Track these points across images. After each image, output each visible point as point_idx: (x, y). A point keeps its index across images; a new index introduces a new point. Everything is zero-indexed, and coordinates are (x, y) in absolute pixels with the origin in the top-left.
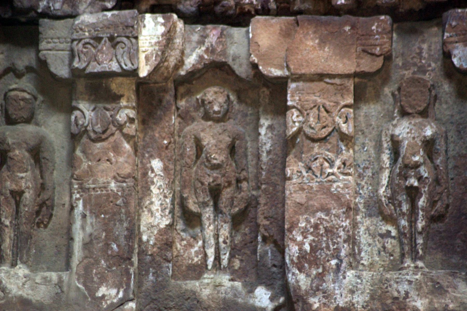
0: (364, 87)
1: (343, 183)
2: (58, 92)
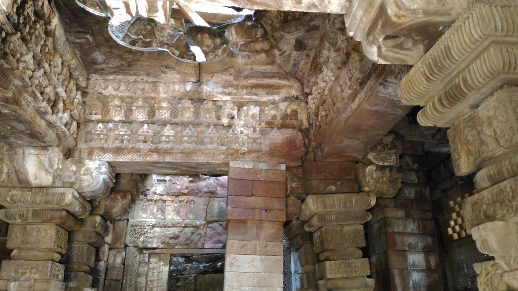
0: (173, 201)
1: (170, 209)
2: (148, 201)
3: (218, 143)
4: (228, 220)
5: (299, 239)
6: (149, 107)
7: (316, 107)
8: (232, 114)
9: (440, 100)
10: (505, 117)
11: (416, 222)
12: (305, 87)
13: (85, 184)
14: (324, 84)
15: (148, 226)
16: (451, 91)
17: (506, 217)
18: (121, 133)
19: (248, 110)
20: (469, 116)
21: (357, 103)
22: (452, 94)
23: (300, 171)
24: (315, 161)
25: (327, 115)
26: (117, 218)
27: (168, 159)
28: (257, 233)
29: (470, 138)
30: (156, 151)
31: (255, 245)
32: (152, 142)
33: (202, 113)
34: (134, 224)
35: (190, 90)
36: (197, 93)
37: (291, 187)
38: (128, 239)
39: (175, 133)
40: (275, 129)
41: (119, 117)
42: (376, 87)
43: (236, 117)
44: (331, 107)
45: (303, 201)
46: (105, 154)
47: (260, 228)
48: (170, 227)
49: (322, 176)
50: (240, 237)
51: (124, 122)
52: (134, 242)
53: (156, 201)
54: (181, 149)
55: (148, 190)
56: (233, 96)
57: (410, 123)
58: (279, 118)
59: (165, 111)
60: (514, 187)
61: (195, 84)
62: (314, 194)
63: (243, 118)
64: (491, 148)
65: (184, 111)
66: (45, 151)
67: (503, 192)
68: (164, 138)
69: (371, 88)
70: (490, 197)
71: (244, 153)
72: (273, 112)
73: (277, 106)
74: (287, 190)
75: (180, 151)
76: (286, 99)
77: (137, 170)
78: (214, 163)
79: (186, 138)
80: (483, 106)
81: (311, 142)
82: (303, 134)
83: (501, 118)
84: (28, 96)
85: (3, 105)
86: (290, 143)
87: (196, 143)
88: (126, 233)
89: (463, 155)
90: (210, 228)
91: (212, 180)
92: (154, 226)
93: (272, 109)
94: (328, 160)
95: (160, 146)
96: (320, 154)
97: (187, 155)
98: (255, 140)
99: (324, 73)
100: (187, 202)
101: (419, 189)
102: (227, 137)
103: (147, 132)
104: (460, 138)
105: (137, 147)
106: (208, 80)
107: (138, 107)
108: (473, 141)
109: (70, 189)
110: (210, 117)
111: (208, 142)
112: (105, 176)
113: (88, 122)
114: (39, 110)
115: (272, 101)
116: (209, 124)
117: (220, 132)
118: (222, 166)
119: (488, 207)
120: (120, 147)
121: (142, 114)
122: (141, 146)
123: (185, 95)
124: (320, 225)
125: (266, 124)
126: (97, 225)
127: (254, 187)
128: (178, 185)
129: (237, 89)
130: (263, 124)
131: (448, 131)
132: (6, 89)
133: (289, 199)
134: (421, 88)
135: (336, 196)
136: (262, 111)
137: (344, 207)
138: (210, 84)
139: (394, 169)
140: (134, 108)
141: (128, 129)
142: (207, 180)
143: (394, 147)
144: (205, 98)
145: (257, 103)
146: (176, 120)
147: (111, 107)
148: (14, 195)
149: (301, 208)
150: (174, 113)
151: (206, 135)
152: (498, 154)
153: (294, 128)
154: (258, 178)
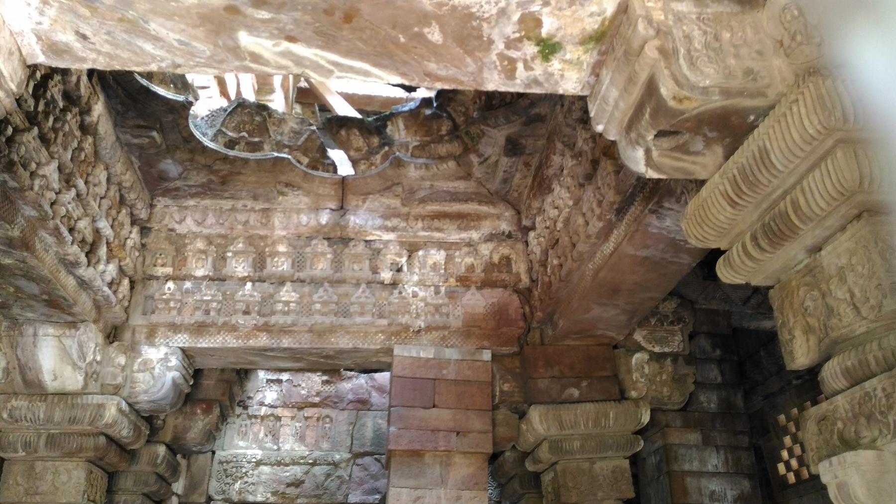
0: (293, 418)
1: (288, 432)
2: (250, 417)
3: (373, 315)
4: (390, 451)
5: (516, 485)
6: (255, 253)
7: (542, 252)
8: (397, 264)
9: (754, 238)
10: (867, 266)
11: (722, 452)
12: (523, 218)
13: (140, 387)
14: (556, 212)
15: (249, 462)
16: (772, 223)
17: (879, 443)
18: (205, 298)
19: (425, 256)
20: (806, 266)
21: (612, 244)
22: (775, 228)
23: (517, 363)
24: (542, 344)
25: (561, 265)
26: (194, 449)
27: (286, 342)
28: (441, 474)
29: (808, 303)
30: (266, 328)
31: (439, 498)
32: (259, 313)
33: (347, 263)
34: (224, 460)
35: (327, 223)
36: (338, 228)
37: (501, 391)
38: (214, 487)
39: (300, 298)
40: (473, 289)
41: (202, 270)
42: (645, 216)
43: (405, 268)
44: (568, 250)
45: (522, 415)
46: (176, 334)
47: (447, 464)
48: (287, 465)
49: (556, 371)
50: (412, 482)
51: (212, 279)
52: (224, 492)
53: (263, 418)
54: (309, 324)
55: (250, 398)
56: (399, 233)
57: (705, 278)
58: (479, 270)
59: (283, 259)
60: (889, 390)
61: (335, 213)
62: (541, 403)
63: (417, 270)
64: (845, 321)
65: (315, 260)
66: (73, 331)
67: (871, 399)
68: (279, 307)
69: (636, 220)
70: (847, 407)
71: (419, 331)
72: (469, 260)
73: (476, 250)
74: (494, 397)
75: (307, 329)
76: (490, 238)
77: (232, 363)
78: (366, 350)
79: (318, 306)
80: (828, 248)
81: (534, 311)
82: (522, 297)
83: (860, 268)
84: (47, 236)
85: (4, 251)
86: (499, 314)
87: (335, 315)
88: (210, 476)
89: (798, 333)
90: (358, 465)
91: (362, 380)
92: (259, 463)
93: (468, 254)
94: (566, 343)
95: (273, 320)
96: (550, 332)
97: (320, 335)
98: (437, 308)
99: (555, 193)
100: (318, 419)
101: (724, 393)
102: (390, 304)
103: (251, 296)
104: (791, 304)
105: (233, 322)
106: (357, 206)
107: (236, 253)
108: (815, 308)
109: (115, 397)
110: (360, 269)
111: (355, 312)
112: (176, 374)
113: (150, 280)
114: (65, 259)
115: (467, 241)
116: (358, 280)
117: (377, 294)
118: (381, 355)
119: (845, 425)
120: (203, 322)
121: (243, 265)
122: (241, 320)
123: (318, 232)
124: (554, 459)
125: (457, 281)
126: (159, 461)
127: (437, 390)
128: (303, 388)
129: (407, 220)
130: (452, 281)
131: (771, 291)
132: (11, 222)
133: (497, 412)
134: (722, 218)
135: (581, 408)
136: (449, 259)
137: (595, 426)
138: (361, 212)
139: (681, 359)
140: (230, 254)
141: (219, 290)
142: (355, 379)
143: (679, 320)
144: (352, 236)
145: (441, 245)
146: (302, 275)
147: (190, 254)
148: (16, 409)
149: (519, 428)
150: (298, 263)
151: (353, 299)
152: (858, 333)
153: (505, 287)
154: (443, 375)
